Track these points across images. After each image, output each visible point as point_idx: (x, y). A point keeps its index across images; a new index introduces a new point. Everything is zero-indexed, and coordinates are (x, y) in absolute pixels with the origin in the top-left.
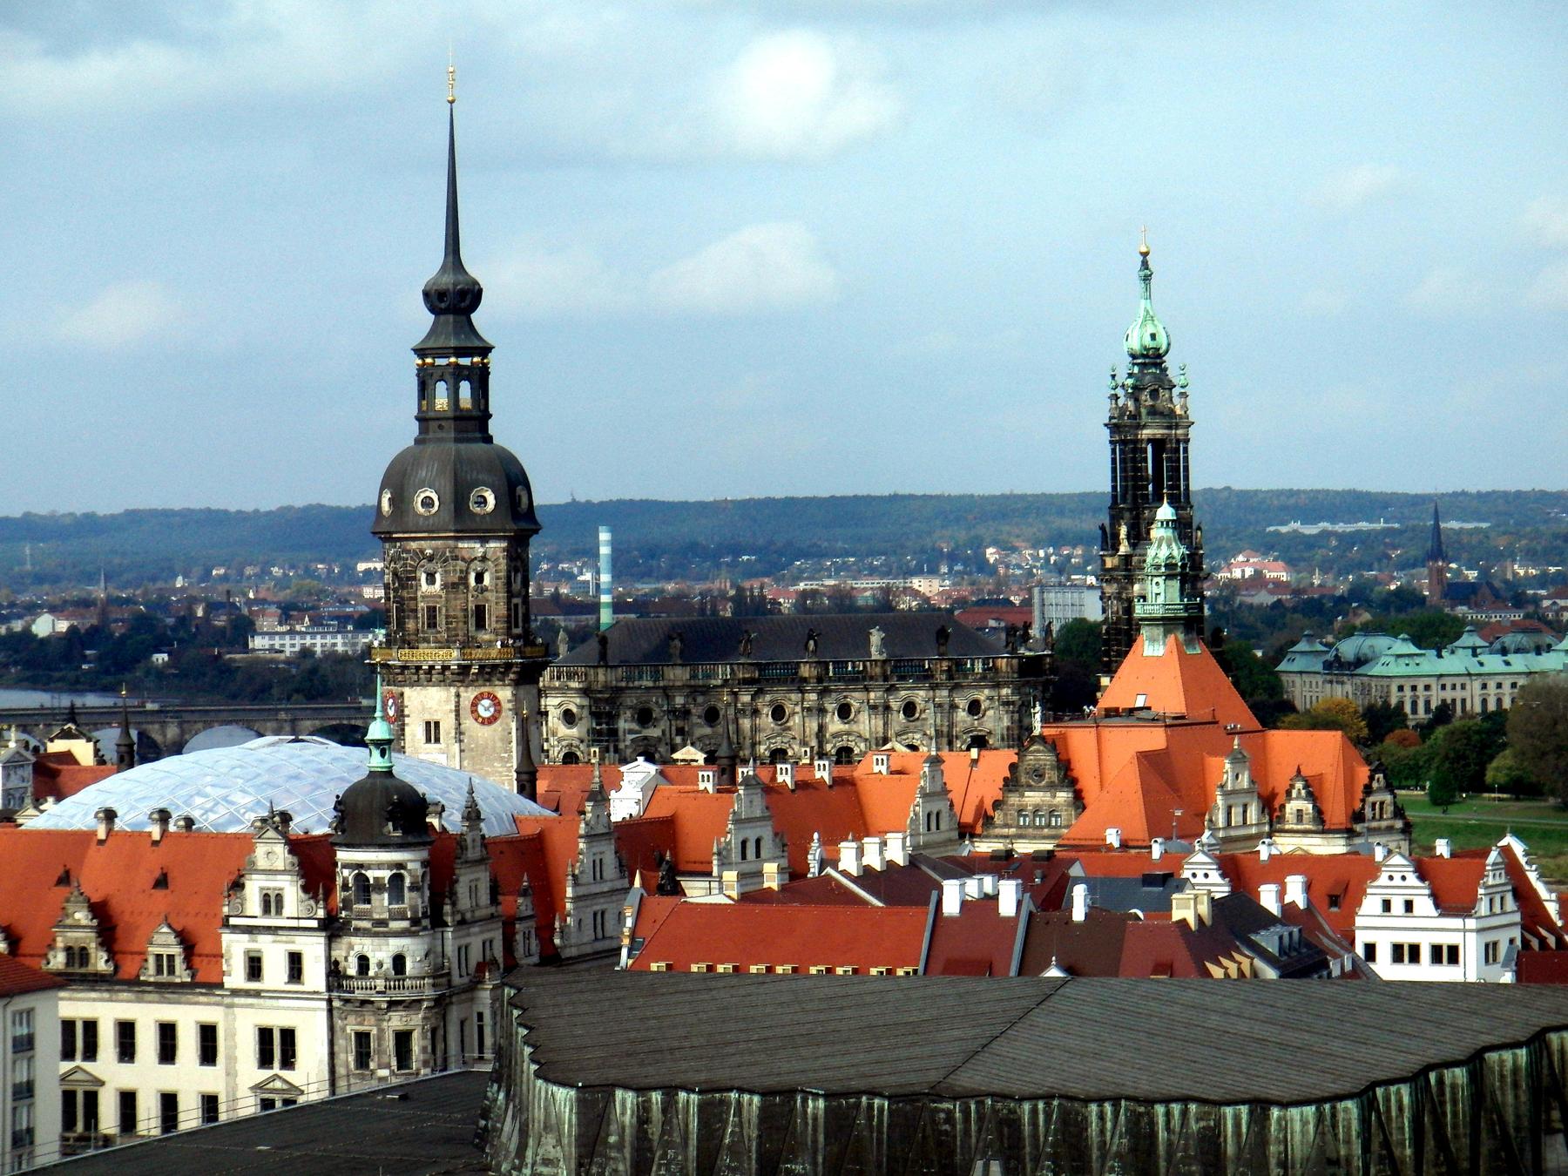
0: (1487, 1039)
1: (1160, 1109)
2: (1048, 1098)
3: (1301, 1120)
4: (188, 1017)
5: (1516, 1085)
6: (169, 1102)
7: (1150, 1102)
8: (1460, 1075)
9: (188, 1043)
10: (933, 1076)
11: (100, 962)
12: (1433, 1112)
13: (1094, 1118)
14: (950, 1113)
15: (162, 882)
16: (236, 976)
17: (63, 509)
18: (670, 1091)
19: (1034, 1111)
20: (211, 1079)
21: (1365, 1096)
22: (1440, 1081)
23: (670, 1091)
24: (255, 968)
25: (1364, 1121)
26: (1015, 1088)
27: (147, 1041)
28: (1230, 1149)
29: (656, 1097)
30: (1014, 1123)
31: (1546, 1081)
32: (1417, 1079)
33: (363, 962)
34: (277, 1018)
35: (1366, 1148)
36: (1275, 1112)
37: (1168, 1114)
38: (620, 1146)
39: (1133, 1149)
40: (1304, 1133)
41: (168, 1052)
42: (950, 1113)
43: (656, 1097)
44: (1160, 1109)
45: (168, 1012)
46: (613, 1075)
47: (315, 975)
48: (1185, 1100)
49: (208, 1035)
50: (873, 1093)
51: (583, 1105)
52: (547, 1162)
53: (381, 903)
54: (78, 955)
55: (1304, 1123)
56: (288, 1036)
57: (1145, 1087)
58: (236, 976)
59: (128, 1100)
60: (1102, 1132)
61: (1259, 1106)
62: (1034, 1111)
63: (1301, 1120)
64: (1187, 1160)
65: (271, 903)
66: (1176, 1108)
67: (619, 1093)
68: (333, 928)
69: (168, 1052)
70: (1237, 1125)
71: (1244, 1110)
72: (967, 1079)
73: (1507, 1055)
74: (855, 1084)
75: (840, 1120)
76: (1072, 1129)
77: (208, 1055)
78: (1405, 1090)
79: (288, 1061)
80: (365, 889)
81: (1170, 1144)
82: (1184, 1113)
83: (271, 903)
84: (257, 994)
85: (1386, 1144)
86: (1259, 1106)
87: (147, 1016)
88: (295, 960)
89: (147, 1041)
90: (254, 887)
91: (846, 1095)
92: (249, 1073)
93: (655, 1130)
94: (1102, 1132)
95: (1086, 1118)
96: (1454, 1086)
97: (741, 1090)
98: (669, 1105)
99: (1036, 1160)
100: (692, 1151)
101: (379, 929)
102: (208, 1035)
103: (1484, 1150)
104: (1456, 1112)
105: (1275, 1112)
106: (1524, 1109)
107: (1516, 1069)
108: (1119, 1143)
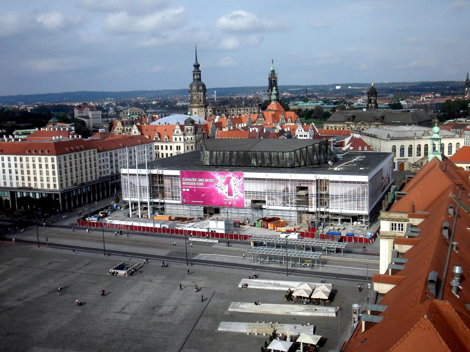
0: (308, 145)
1: (272, 153)
2: (260, 152)
3: (287, 154)
4: (169, 145)
5: (311, 150)
6: (167, 154)
7: (271, 152)
8: (305, 149)
9: (169, 148)
10: (248, 149)
11: (159, 139)
12: (302, 153)
13: (265, 154)
14: (249, 153)
15: (165, 130)
16: (174, 140)
17: (115, 91)
18: (219, 151)
19: (259, 153)
20: (171, 152)
21: (295, 151)
22: (303, 150)
23: (219, 151)
24: (176, 139)
25: (294, 154)
26: (257, 151)
27: (164, 148)
28: (280, 157)
29: (218, 152)
30: (256, 154)
31: (314, 149)
32: (300, 149)
33: (188, 138)
34: (178, 145)
35: (295, 157)
36: (285, 153)
37: (273, 153)
38: (214, 158)
39: (269, 157)
40: (288, 155)
41: (167, 149)
42: (249, 153)
43: (218, 152)
44: (272, 153)
45: (167, 144)
46: (213, 150)
47: (182, 140)
48: (275, 152)
49: (171, 147)
50: (241, 151)
51: (210, 153)
52: (206, 160)
53: (189, 132)
54: (156, 138)
55: (288, 154)
56: (180, 147)
57: (270, 150)
58: (174, 140)
59: (162, 154)
60: (266, 155)
61: (283, 152)
62: (259, 153)
63: (287, 154)
64: (275, 158)
65: (178, 132)
66: (274, 153)
67: (214, 152)
68: (184, 135)
69: (167, 149)
70: (281, 154)
71: (281, 153)
72: (252, 150)
73: (310, 147)
74: (239, 150)
75: (238, 154)
76: (263, 155)
77: (171, 149)
78: (299, 151)
79: (180, 150)
80: (188, 130)
81: (273, 157)
82: (275, 153)
83: (178, 132)
84: (176, 142)
85: (297, 156)
86: (283, 152)
87: (164, 145)
88: (180, 138)
89: (164, 148)
90: (176, 131)
91: (238, 152)
92: (176, 151)
93: (218, 156)
94: (266, 155)
95: (264, 154)
96: (304, 150)
97: (227, 151)
98: (219, 153)
99: (259, 158)
100: (222, 158)
101: (189, 135)
102: (171, 147)
103: (307, 157)
104: (304, 153)
105: (285, 153)
106: (312, 153)
107: (311, 148)
108: (268, 157)
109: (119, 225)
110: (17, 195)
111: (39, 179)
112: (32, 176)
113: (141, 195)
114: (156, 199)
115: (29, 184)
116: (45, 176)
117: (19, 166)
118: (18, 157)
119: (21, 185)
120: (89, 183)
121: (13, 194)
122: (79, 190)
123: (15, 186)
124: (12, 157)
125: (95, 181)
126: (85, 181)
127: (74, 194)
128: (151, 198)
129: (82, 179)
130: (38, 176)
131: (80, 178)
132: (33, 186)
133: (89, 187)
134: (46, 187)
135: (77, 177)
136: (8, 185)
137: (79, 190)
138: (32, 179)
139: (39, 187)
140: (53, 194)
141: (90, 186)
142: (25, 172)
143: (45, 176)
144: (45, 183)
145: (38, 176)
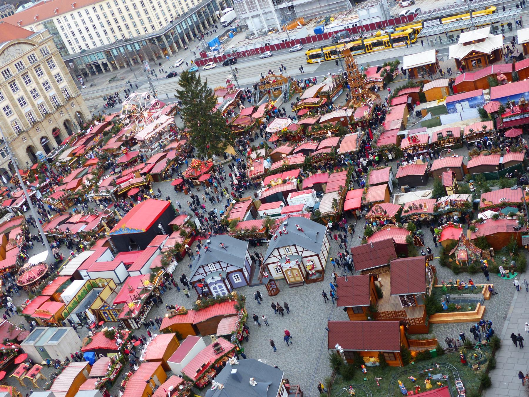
109: (246, 51)
110: (113, 53)
111: (131, 25)
112: (121, 24)
113: (260, 6)
114: (281, 3)
115: (123, 35)
116: (136, 19)
117: (102, 17)
118: (97, 6)
119: (113, 40)
120: (192, 10)
121: (108, 53)
122: (183, 23)
123: (106, 43)
124: (90, 9)
125: (198, 7)
126: (186, 10)
127: (180, 31)
128: (275, 5)
129: (182, 8)
130: (129, 22)
131: (178, 8)
132: (127, 36)
133: (194, 16)
134: (143, 33)
135: (175, 7)
136: (99, 45)
137: (183, 23)
138: (123, 28)
139: (135, 35)
140: (155, 39)
141: (195, 13)
142: (112, 22)
143: (136, 19)
144: (140, 27)
145: (129, 22)
